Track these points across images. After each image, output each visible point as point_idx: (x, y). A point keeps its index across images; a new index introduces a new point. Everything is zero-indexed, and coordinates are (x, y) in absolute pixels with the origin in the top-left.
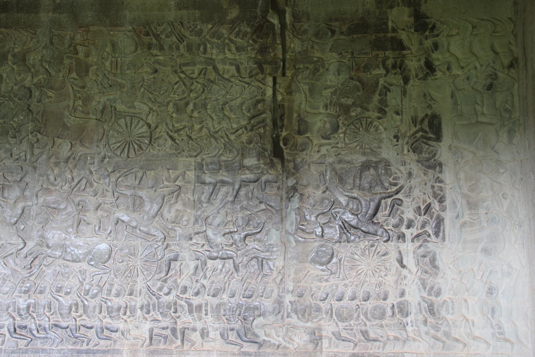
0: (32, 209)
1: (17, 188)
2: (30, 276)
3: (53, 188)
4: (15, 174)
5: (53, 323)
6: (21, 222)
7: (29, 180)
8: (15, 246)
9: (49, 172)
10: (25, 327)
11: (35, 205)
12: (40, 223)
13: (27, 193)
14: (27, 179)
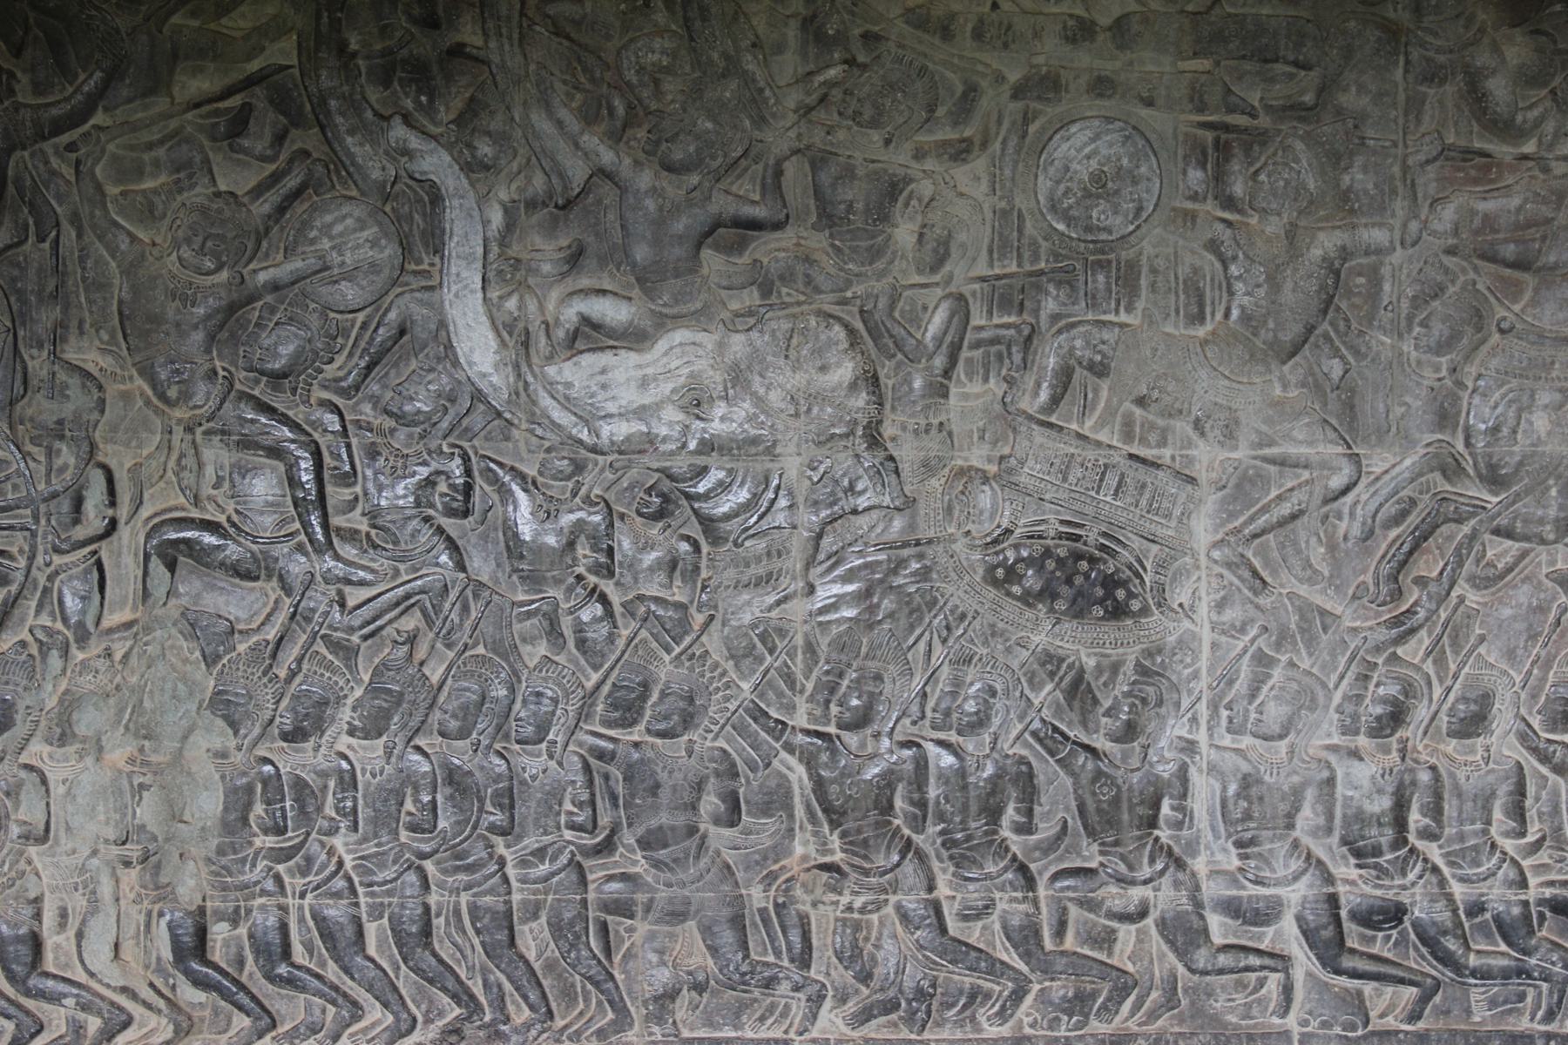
0: (1386, 271)
1: (1299, 146)
2: (1401, 639)
3: (1503, 150)
4: (1280, 68)
5: (1548, 892)
6: (1327, 337)
7: (1365, 101)
8: (1306, 475)
9: (1483, 59)
10: (1396, 913)
11: (1407, 241)
12: (1441, 348)
13: (1357, 177)
14: (1349, 99)
